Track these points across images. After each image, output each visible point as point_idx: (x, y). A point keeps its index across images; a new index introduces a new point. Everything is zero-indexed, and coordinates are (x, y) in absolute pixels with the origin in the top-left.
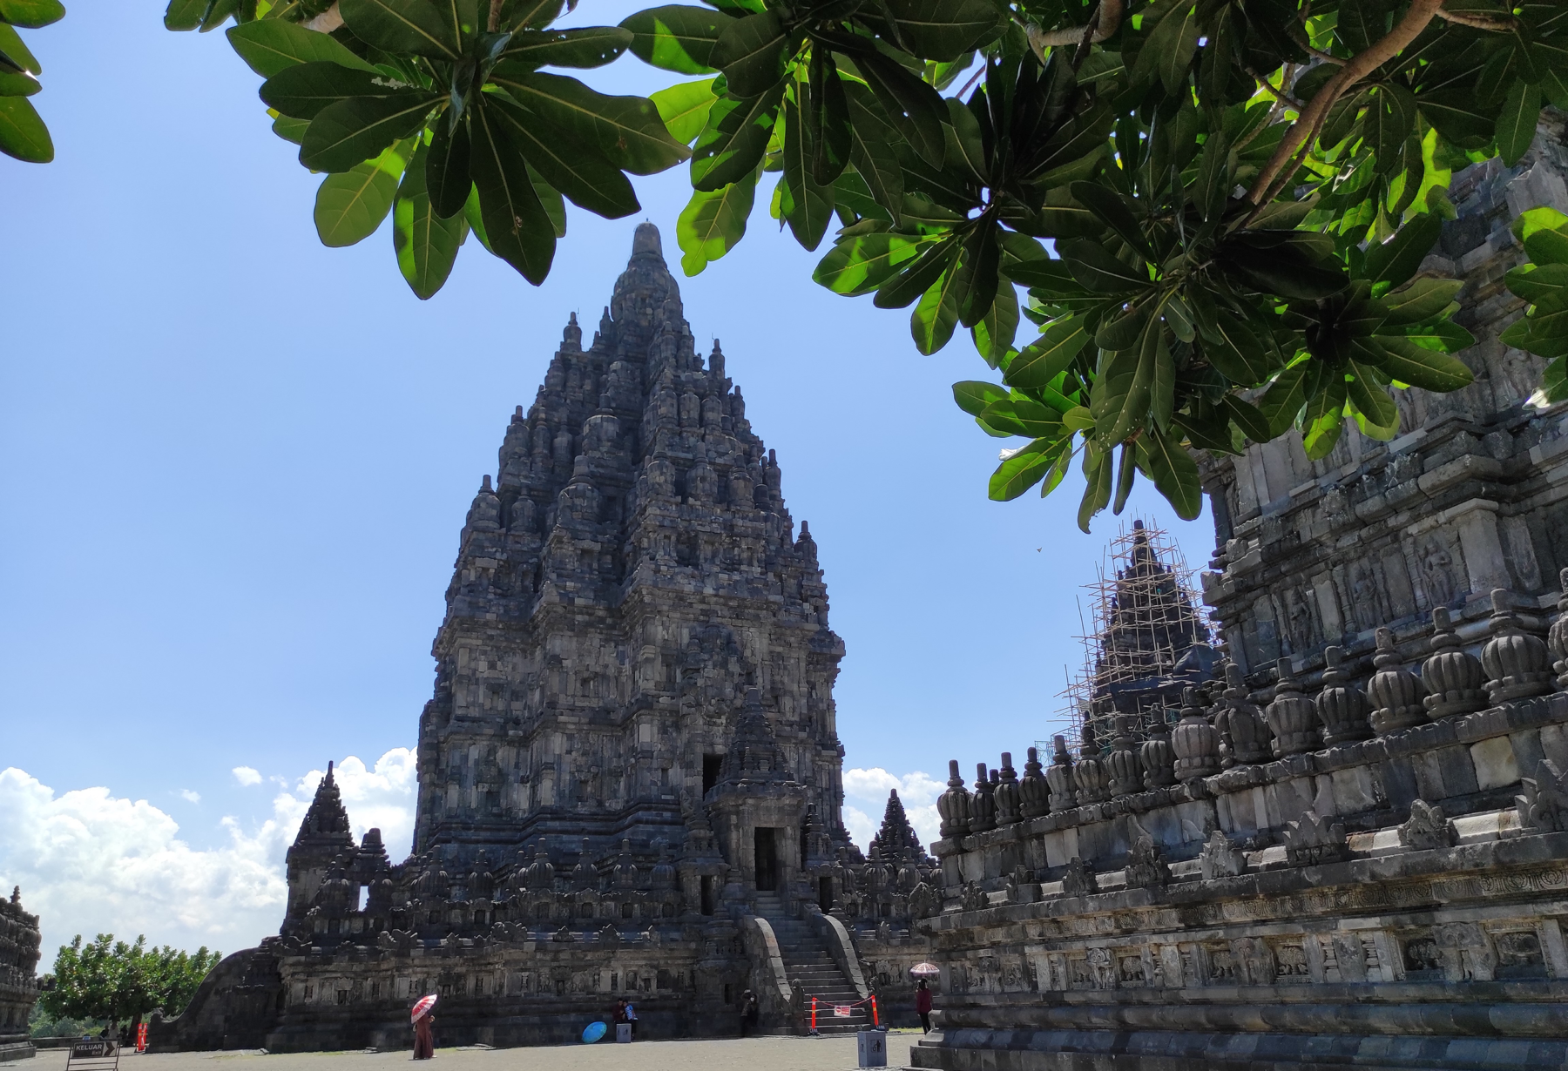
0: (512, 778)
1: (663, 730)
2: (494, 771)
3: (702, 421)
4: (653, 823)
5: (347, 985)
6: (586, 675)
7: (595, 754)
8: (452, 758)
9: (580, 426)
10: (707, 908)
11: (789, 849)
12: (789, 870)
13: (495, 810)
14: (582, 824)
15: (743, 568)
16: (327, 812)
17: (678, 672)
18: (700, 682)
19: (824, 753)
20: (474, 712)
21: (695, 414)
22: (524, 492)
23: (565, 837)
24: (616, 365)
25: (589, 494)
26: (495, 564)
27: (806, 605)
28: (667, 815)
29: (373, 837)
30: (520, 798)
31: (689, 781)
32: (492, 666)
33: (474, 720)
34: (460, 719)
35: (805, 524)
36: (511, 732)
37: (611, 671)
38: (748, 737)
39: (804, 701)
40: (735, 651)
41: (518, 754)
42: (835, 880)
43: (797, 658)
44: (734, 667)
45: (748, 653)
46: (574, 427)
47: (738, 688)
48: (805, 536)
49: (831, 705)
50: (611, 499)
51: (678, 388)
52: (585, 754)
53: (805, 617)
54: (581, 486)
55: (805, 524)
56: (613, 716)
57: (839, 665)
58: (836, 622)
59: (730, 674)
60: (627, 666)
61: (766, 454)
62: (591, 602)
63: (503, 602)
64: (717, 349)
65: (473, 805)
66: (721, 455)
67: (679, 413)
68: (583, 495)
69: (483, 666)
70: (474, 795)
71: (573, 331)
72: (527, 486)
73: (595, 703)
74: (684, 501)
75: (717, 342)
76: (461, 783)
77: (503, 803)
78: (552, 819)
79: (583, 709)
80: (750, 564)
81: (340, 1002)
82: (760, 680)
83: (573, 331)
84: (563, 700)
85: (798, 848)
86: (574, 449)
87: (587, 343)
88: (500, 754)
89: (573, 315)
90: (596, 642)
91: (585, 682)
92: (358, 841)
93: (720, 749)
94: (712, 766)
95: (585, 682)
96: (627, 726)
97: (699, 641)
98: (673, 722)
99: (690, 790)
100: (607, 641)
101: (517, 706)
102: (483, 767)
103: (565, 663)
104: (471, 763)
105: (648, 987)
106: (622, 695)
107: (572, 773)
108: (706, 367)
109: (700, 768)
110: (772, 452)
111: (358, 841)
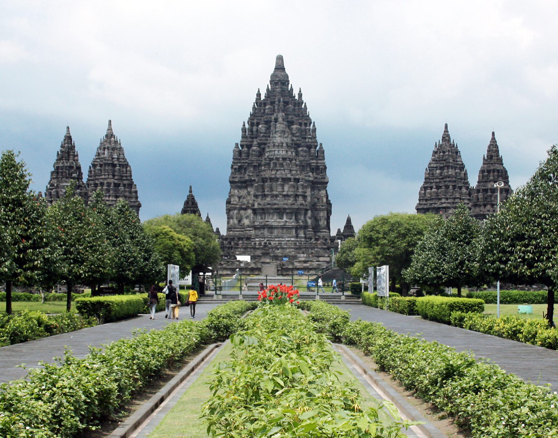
20: (235, 203)
24: (267, 107)
26: (237, 167)
29: (218, 229)
32: (238, 191)
46: (258, 124)
55: (321, 144)
64: (300, 91)
68: (253, 151)
70: (236, 221)
71: (259, 95)
76: (232, 218)
77: (242, 222)
83: (259, 95)
87: (263, 97)
101: (244, 200)
108: (297, 98)
110: (314, 122)
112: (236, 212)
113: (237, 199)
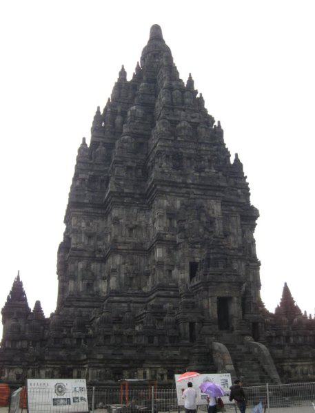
0: (98, 277)
1: (169, 252)
2: (90, 274)
3: (183, 103)
4: (163, 297)
5: (20, 371)
6: (131, 226)
7: (136, 264)
8: (71, 267)
9: (126, 113)
10: (192, 338)
11: (235, 308)
12: (235, 319)
13: (91, 292)
14: (131, 298)
15: (206, 170)
16: (17, 293)
17: (175, 222)
18: (186, 226)
19: (251, 264)
20: (80, 247)
21: (179, 100)
22: (101, 144)
23: (123, 305)
25: (130, 140)
26: (88, 177)
27: (239, 191)
28: (172, 293)
29: (38, 304)
30: (102, 287)
31: (182, 276)
32: (88, 225)
33: (80, 250)
34: (75, 249)
35: (236, 155)
36: (97, 256)
37: (143, 224)
38: (212, 251)
39: (240, 238)
40: (204, 211)
41: (101, 266)
42: (260, 324)
43: (236, 221)
44: (204, 219)
45: (210, 212)
46: (124, 114)
47: (206, 229)
48: (237, 160)
49: (253, 241)
50: (141, 144)
51: (170, 89)
52: (132, 264)
53: (238, 195)
54: (126, 137)
55: (236, 155)
56: (145, 246)
57: (257, 222)
58: (254, 201)
59: (202, 223)
60: (151, 222)
61: (216, 124)
62: (132, 191)
63: (92, 194)
65: (81, 290)
66: (193, 118)
67: (172, 100)
68: (126, 142)
69: (83, 224)
70: (81, 286)
71: (123, 73)
72: (102, 142)
73: (137, 240)
74: (176, 138)
75: (190, 75)
77: (95, 289)
78: (116, 296)
79: (130, 243)
80: (210, 168)
81: (18, 379)
82: (217, 226)
83: (123, 73)
84: (120, 239)
85: (240, 308)
86: (123, 122)
87: (129, 78)
88: (92, 267)
89: (123, 66)
90: (135, 211)
91: (131, 230)
92: (32, 306)
93: (197, 260)
94: (193, 268)
95: (131, 230)
96: (151, 251)
97: (185, 207)
98: (173, 246)
99: (183, 280)
100: (141, 210)
101: (100, 243)
102: (85, 272)
103: (120, 221)
104: (79, 270)
105: (162, 378)
106: (149, 236)
107: (125, 274)
109: (187, 268)
110: (219, 122)
111: (32, 306)
112: (81, 265)
113: (84, 239)
